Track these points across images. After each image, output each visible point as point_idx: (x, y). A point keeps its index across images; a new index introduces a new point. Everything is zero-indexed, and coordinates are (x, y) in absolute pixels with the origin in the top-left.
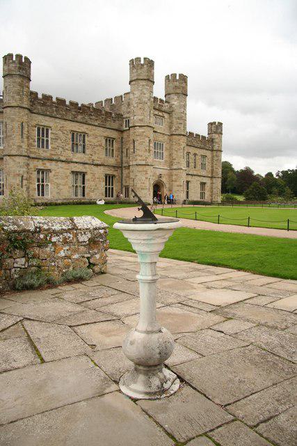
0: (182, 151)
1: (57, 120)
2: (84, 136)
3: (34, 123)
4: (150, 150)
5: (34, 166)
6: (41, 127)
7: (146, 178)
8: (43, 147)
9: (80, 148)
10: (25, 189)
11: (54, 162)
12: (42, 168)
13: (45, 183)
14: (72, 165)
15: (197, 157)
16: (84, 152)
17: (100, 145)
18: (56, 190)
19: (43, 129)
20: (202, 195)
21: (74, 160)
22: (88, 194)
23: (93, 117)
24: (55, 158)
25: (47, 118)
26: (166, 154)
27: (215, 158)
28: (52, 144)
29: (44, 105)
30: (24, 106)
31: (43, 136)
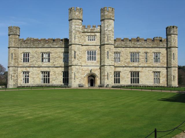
0: (106, 54)
1: (33, 49)
2: (49, 54)
3: (22, 52)
4: (75, 58)
5: (21, 70)
6: (25, 53)
7: (72, 73)
8: (26, 62)
9: (47, 60)
10: (12, 80)
11: (31, 68)
12: (26, 71)
13: (27, 78)
14: (41, 68)
15: (149, 55)
16: (49, 61)
17: (59, 57)
18: (33, 80)
19: (26, 54)
20: (157, 79)
21: (43, 66)
22: (51, 82)
23: (55, 44)
24: (32, 66)
25: (28, 49)
26: (98, 57)
27: (169, 53)
28: (30, 60)
29: (26, 43)
30: (12, 46)
31: (26, 57)
